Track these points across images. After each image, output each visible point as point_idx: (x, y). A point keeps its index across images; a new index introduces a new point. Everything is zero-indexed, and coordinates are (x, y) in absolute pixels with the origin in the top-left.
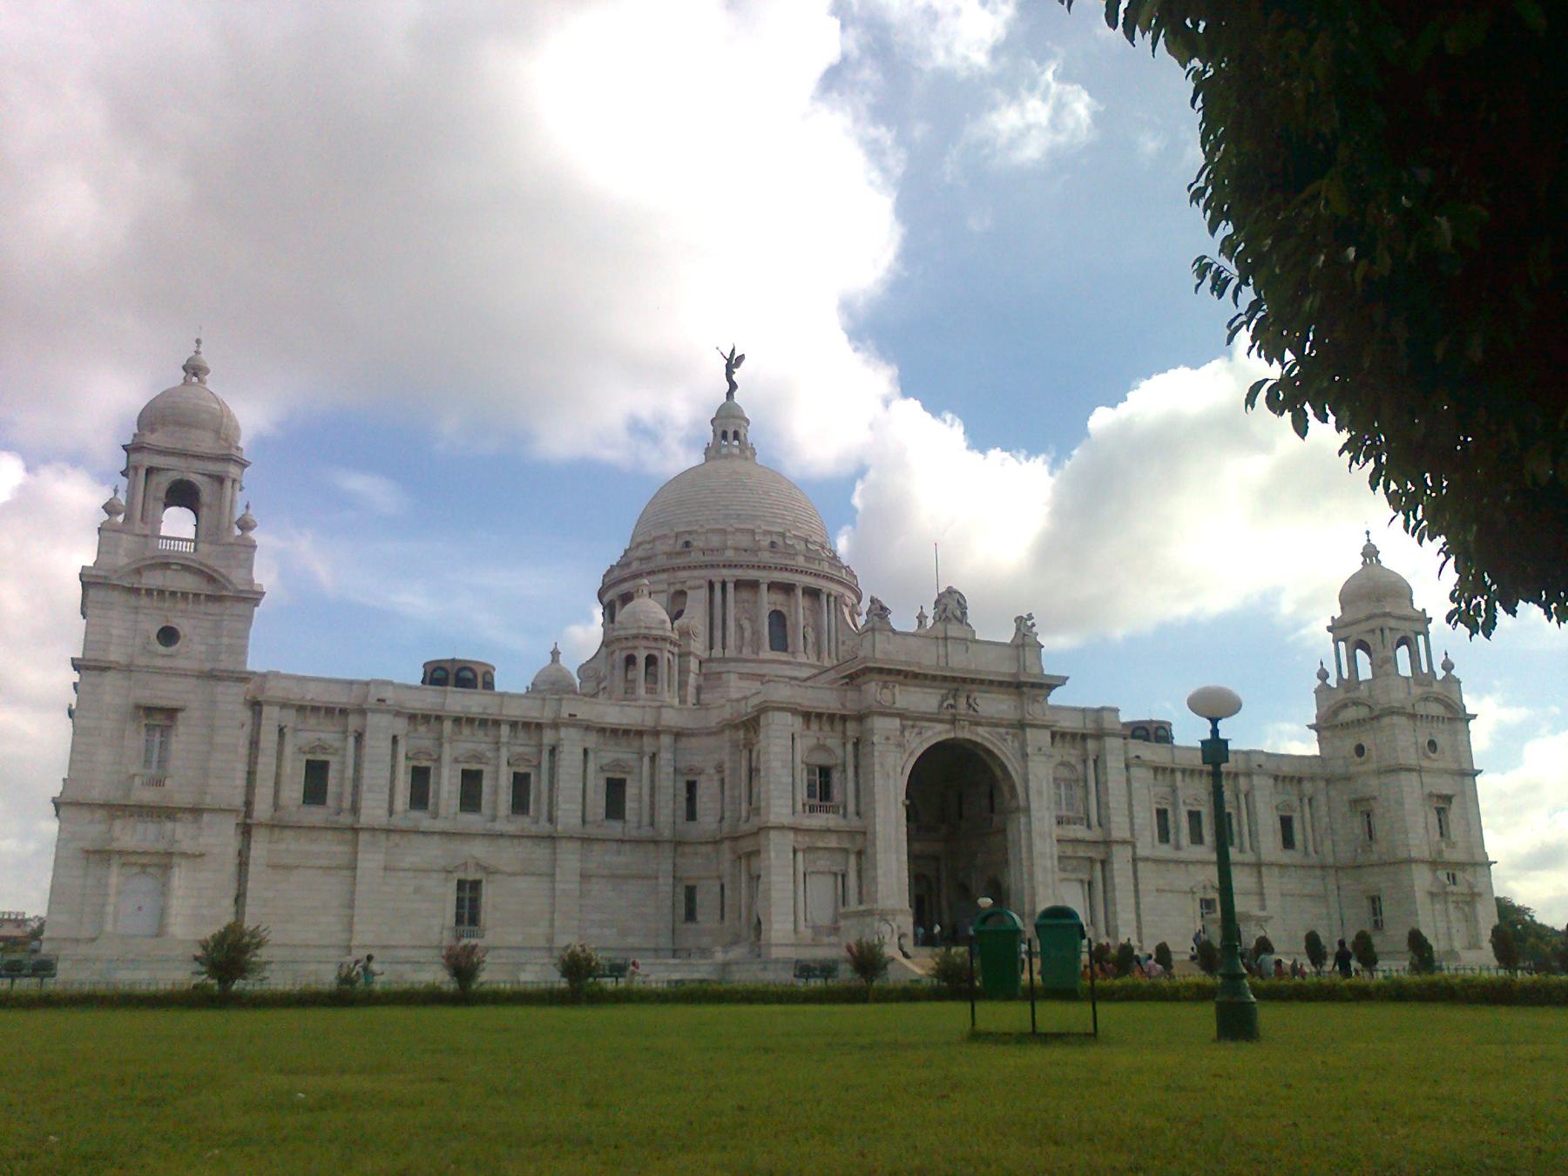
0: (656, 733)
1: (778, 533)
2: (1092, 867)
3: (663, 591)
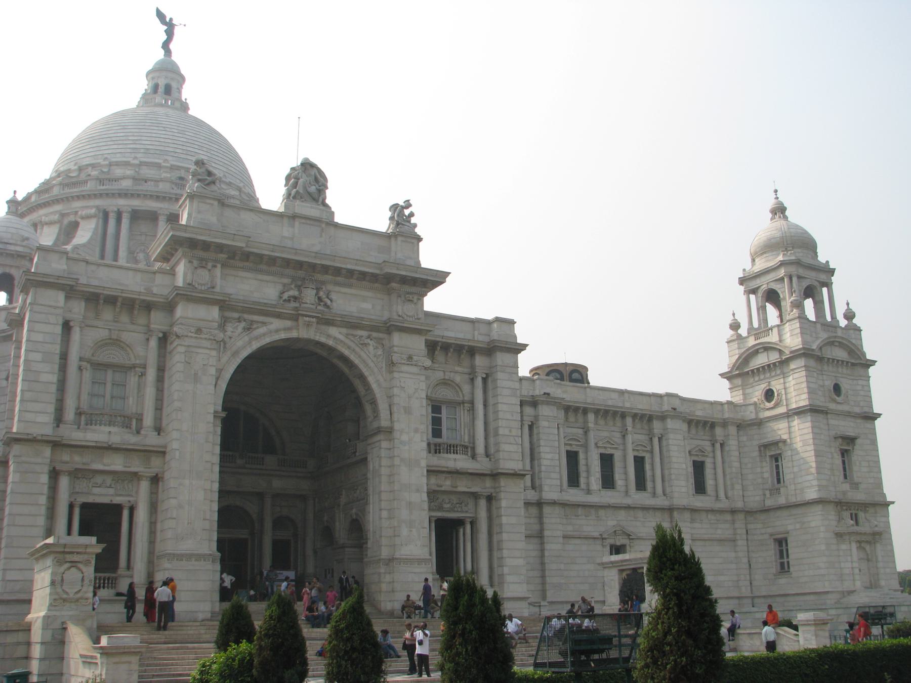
2: (476, 505)
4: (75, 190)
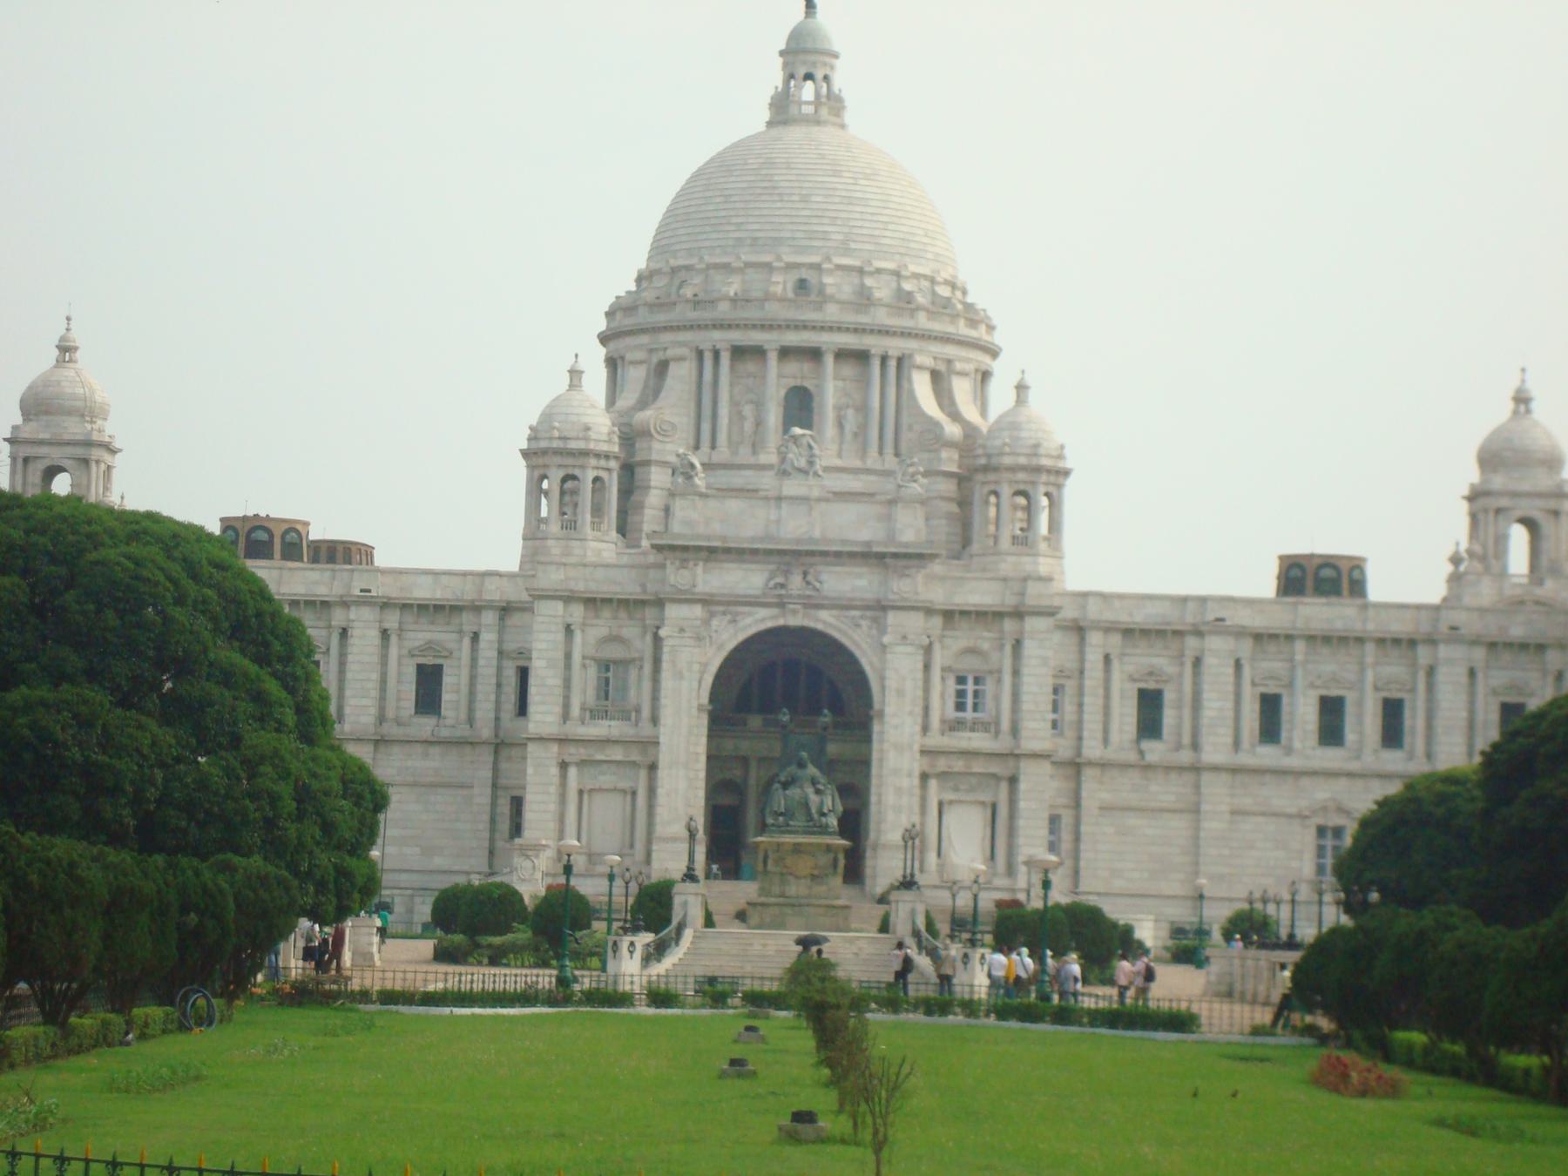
0: (477, 608)
1: (812, 266)
3: (641, 362)
4: (661, 318)
